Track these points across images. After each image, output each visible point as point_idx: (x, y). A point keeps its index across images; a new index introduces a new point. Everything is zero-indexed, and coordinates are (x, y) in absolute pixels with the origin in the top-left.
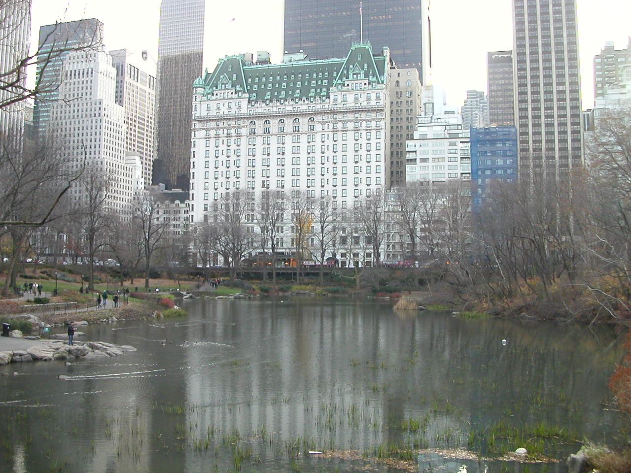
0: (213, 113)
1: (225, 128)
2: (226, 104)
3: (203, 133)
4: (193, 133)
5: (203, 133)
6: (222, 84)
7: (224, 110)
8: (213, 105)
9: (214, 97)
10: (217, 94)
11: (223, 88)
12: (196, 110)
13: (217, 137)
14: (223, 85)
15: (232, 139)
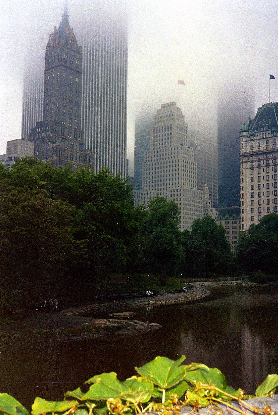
0: (256, 149)
1: (265, 159)
2: (265, 142)
3: (248, 165)
4: (241, 165)
5: (248, 165)
6: (262, 127)
7: (263, 147)
8: (255, 144)
9: (256, 138)
10: (258, 135)
11: (262, 130)
12: (243, 148)
13: (259, 167)
14: (262, 128)
15: (271, 167)
